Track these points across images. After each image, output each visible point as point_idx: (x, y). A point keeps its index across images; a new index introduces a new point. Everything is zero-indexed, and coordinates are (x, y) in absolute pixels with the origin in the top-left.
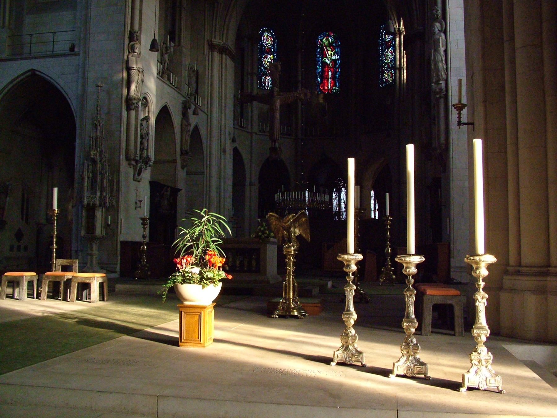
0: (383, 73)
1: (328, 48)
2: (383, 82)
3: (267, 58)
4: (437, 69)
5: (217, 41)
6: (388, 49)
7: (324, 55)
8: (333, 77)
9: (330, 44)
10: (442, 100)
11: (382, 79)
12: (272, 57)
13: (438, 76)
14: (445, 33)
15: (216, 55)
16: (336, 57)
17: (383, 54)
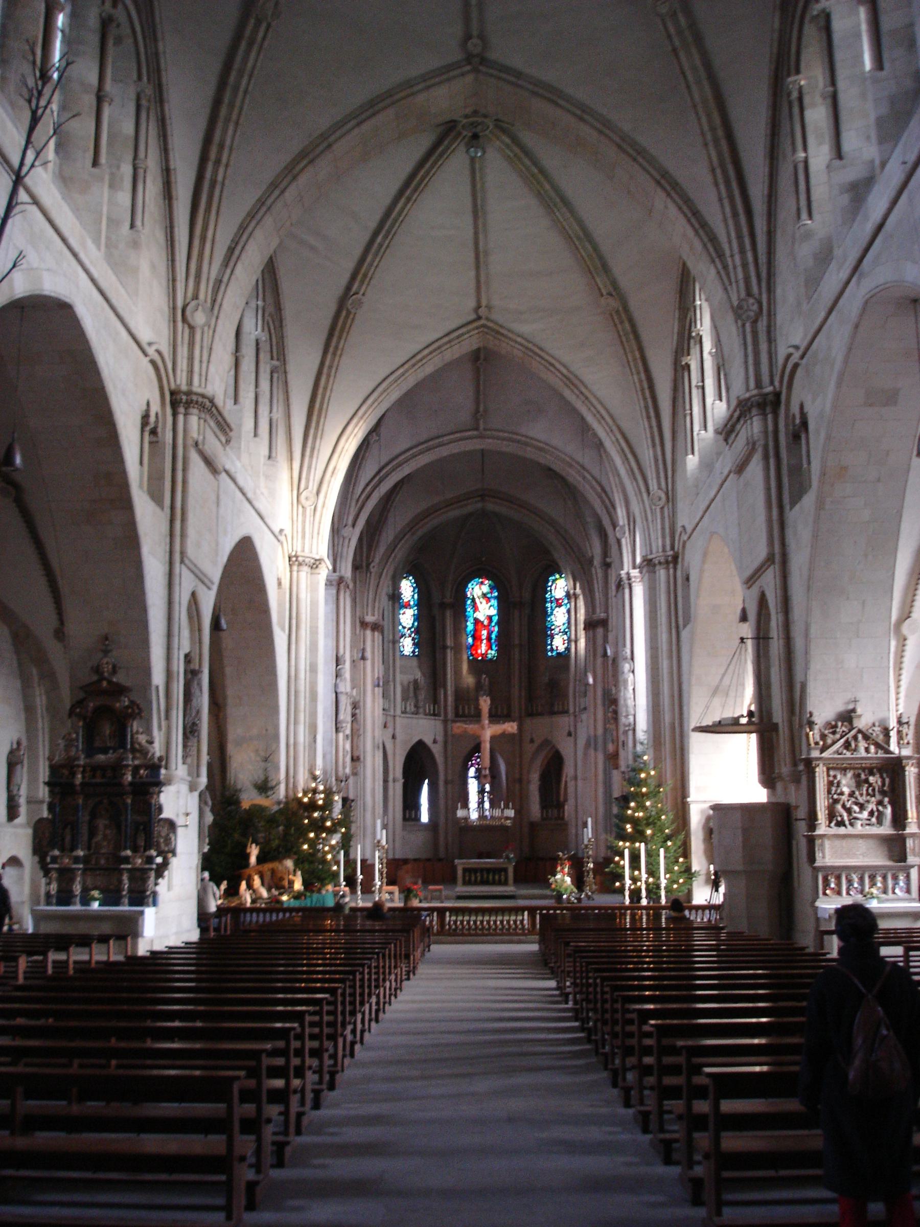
1: (481, 599)
2: (552, 650)
3: (404, 613)
4: (627, 706)
5: (369, 619)
6: (560, 605)
7: (475, 608)
8: (489, 638)
9: (484, 595)
10: (630, 733)
11: (551, 645)
13: (627, 711)
14: (633, 672)
15: (369, 633)
17: (552, 614)
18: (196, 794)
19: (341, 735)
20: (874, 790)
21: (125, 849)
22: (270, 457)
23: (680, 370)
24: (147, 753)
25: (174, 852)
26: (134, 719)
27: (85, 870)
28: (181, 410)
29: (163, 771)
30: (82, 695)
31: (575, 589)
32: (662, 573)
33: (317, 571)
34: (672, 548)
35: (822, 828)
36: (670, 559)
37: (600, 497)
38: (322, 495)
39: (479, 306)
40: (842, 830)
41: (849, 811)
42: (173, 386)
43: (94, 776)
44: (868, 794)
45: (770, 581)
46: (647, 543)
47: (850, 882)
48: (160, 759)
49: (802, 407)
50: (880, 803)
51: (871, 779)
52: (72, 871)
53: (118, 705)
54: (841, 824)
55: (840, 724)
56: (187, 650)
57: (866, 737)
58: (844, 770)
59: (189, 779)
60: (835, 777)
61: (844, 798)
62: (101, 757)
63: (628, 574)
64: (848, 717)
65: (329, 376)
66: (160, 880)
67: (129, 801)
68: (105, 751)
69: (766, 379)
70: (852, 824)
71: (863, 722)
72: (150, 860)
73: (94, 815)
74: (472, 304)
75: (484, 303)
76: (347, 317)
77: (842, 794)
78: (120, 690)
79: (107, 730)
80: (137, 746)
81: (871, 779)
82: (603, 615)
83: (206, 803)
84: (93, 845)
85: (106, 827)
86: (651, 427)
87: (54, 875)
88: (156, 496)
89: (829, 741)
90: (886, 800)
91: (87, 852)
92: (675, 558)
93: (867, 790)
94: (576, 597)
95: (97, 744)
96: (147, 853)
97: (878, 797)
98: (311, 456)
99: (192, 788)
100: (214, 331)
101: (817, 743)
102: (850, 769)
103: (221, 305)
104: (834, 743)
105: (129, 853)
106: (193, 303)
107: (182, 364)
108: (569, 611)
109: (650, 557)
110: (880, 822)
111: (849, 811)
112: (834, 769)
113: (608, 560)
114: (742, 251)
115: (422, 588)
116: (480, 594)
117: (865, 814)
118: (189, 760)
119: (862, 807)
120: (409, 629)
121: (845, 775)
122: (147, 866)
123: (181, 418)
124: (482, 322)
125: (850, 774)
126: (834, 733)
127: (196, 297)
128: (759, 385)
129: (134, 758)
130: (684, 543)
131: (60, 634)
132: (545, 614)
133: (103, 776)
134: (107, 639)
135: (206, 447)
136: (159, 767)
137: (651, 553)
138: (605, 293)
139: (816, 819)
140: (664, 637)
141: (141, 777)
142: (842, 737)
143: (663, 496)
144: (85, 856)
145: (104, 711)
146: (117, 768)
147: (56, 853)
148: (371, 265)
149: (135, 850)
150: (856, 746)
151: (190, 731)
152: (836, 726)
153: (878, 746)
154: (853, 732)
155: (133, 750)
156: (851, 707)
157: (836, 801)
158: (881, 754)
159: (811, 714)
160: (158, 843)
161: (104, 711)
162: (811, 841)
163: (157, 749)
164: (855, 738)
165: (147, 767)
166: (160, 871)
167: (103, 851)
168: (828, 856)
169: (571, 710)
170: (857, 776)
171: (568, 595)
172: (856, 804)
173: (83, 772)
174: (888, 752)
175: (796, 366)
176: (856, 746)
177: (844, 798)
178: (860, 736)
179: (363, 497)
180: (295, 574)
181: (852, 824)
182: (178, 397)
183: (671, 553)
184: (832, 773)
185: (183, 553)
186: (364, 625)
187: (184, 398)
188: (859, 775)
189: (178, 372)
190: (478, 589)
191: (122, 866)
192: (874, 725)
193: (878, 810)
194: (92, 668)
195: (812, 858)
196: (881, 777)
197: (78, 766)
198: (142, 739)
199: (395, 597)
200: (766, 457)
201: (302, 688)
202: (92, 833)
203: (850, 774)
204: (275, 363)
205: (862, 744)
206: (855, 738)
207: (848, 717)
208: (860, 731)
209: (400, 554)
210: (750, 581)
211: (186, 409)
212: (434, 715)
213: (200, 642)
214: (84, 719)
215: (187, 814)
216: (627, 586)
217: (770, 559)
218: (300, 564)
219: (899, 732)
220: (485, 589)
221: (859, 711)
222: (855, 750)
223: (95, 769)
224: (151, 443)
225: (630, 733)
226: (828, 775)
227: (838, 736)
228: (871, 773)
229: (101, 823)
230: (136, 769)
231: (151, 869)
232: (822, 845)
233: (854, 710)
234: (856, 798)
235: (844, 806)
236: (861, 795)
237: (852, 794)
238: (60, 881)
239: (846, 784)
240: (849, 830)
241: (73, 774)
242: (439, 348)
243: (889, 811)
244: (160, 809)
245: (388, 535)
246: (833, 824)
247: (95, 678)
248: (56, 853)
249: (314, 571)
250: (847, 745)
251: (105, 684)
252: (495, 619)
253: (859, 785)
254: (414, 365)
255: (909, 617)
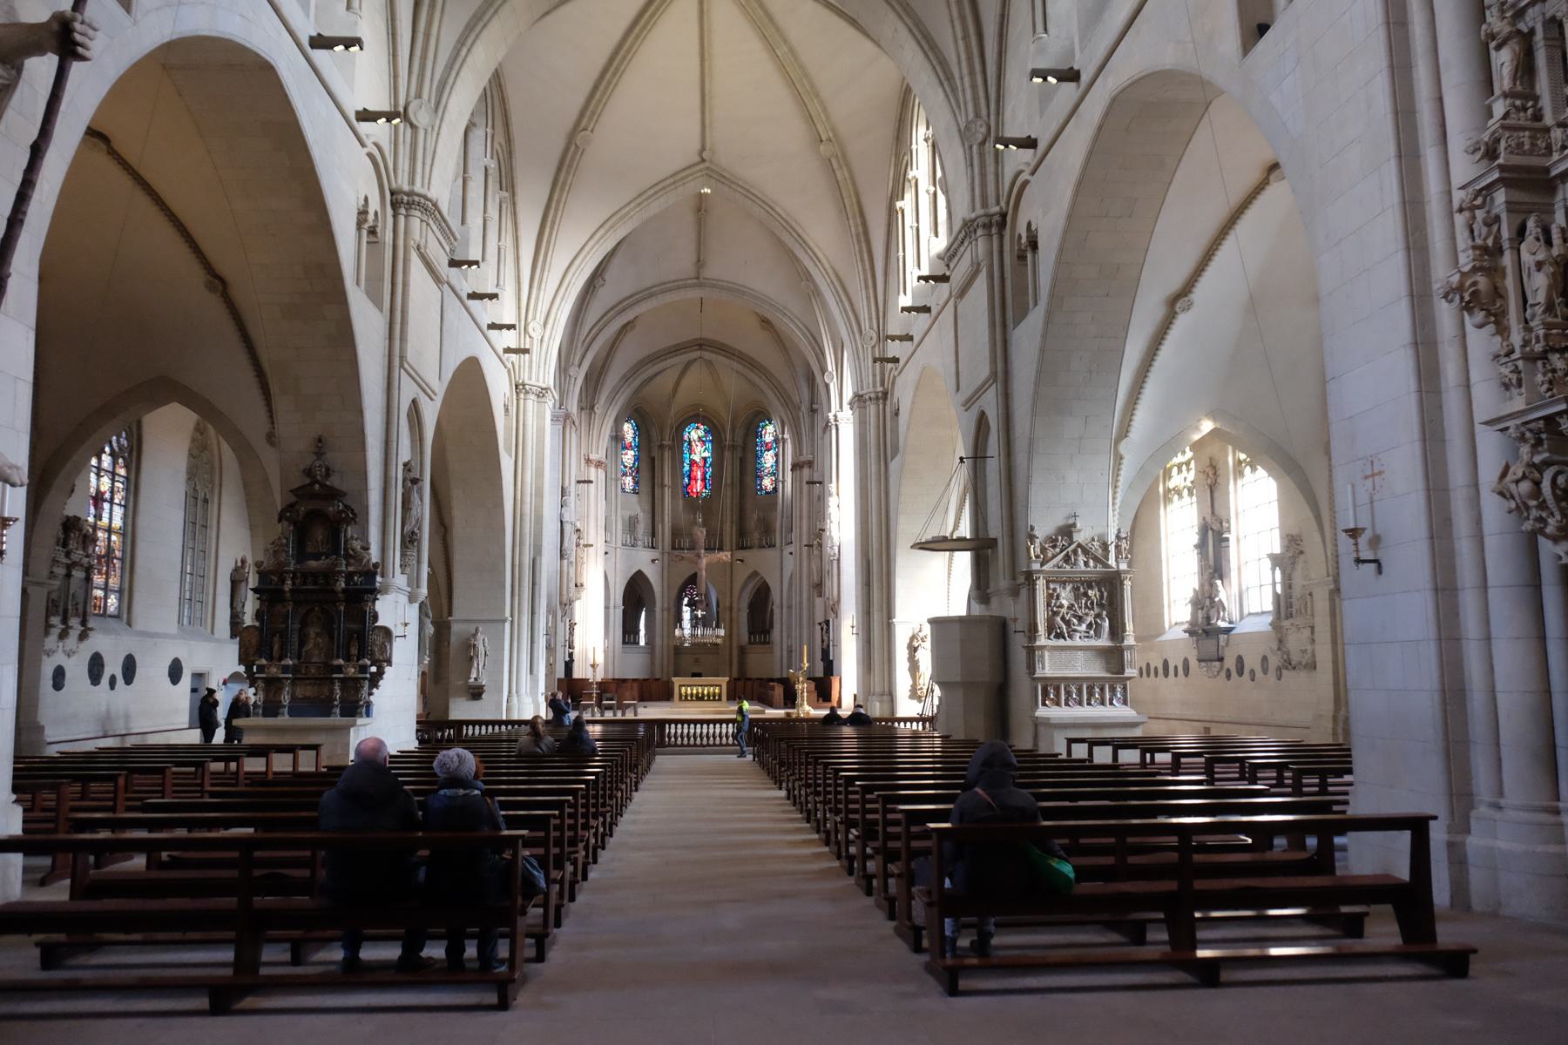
0: (762, 478)
2: (761, 489)
5: (593, 456)
6: (769, 450)
7: (691, 451)
8: (704, 479)
10: (835, 563)
11: (761, 485)
12: (632, 453)
15: (593, 470)
16: (707, 454)
18: (416, 606)
19: (565, 562)
20: (1092, 603)
21: (338, 657)
22: (497, 285)
23: (892, 215)
24: (361, 560)
25: (389, 663)
26: (348, 524)
27: (294, 681)
28: (403, 211)
29: (379, 579)
30: (293, 499)
31: (783, 433)
32: (872, 409)
33: (543, 400)
34: (882, 384)
35: (1042, 641)
36: (880, 395)
37: (810, 344)
38: (549, 326)
39: (703, 149)
40: (1061, 642)
41: (1068, 623)
42: (394, 186)
43: (305, 583)
44: (1086, 607)
45: (990, 403)
46: (859, 380)
47: (1068, 693)
48: (376, 565)
49: (1029, 224)
50: (1098, 616)
51: (1090, 592)
52: (279, 680)
53: (331, 509)
54: (1060, 636)
55: (1060, 538)
56: (406, 459)
57: (1086, 552)
58: (1064, 583)
59: (409, 589)
60: (1054, 590)
61: (1064, 610)
62: (313, 564)
63: (835, 416)
64: (1067, 531)
65: (557, 210)
66: (375, 690)
67: (342, 608)
68: (317, 557)
69: (992, 200)
70: (1070, 637)
71: (1080, 538)
72: (364, 669)
73: (304, 624)
74: (698, 146)
75: (708, 147)
76: (575, 153)
77: (1061, 606)
78: (334, 494)
79: (319, 534)
80: (351, 552)
81: (1090, 592)
82: (810, 457)
83: (427, 616)
84: (304, 654)
85: (317, 634)
86: (864, 270)
87: (261, 684)
88: (375, 297)
89: (1050, 555)
90: (1104, 613)
91: (296, 662)
92: (885, 394)
93: (1086, 604)
94: (784, 441)
95: (309, 550)
96: (361, 662)
97: (1097, 610)
98: (539, 288)
99: (412, 599)
100: (438, 134)
101: (1037, 557)
102: (1069, 582)
103: (445, 107)
104: (1054, 556)
105: (341, 662)
106: (418, 101)
107: (404, 164)
108: (777, 455)
109: (861, 393)
110: (1098, 635)
111: (1068, 623)
112: (1053, 582)
113: (815, 406)
114: (972, 73)
115: (640, 430)
116: (696, 437)
117: (1084, 627)
118: (408, 570)
119: (1080, 619)
120: (631, 468)
121: (1064, 588)
122: (360, 676)
123: (402, 219)
124: (707, 164)
125: (1069, 588)
126: (1054, 547)
127: (419, 96)
128: (985, 204)
129: (347, 565)
130: (895, 378)
131: (271, 438)
132: (757, 457)
133: (315, 583)
134: (320, 441)
135: (428, 251)
136: (376, 573)
137: (862, 389)
138: (824, 138)
139: (1036, 630)
140: (873, 468)
141: (356, 584)
142: (1062, 551)
143: (875, 336)
144: (294, 665)
145: (315, 516)
146: (329, 575)
147: (264, 662)
148: (599, 101)
149: (348, 658)
150: (1075, 560)
151: (410, 540)
152: (1057, 540)
153: (1096, 559)
154: (1073, 547)
155: (347, 556)
156: (1071, 521)
157: (1055, 614)
158: (1099, 568)
159: (1032, 528)
160: (373, 653)
161: (315, 516)
162: (1031, 651)
163: (374, 555)
164: (1075, 552)
165: (360, 574)
166: (375, 681)
167: (314, 660)
168: (1048, 668)
169: (778, 544)
170: (1076, 589)
171: (776, 440)
172: (1075, 616)
173: (292, 579)
174: (1106, 566)
175: (1026, 183)
176: (1075, 560)
177: (1064, 610)
178: (1080, 550)
179: (589, 338)
180: (522, 401)
181: (1070, 637)
182: (399, 197)
183: (881, 389)
184: (1052, 586)
185: (402, 358)
186: (588, 461)
187: (405, 198)
188: (1078, 588)
189: (400, 172)
190: (694, 433)
191: (334, 676)
192: (1093, 540)
193: (1096, 622)
194: (304, 471)
195: (1031, 667)
196: (1100, 591)
197: (288, 572)
198: (357, 545)
199: (617, 438)
200: (991, 276)
201: (527, 510)
202: (302, 643)
203: (1069, 588)
204: (505, 194)
205: (1081, 558)
206: (1075, 552)
207: (1067, 531)
208: (1079, 545)
209: (621, 400)
210: (968, 404)
211: (406, 209)
212: (653, 547)
213: (422, 453)
214: (295, 523)
215: (406, 624)
216: (834, 427)
217: (994, 374)
218: (527, 392)
219: (1117, 547)
220: (701, 433)
221: (1079, 526)
222: (1075, 564)
223: (306, 575)
224: (368, 242)
225: (835, 563)
226: (1048, 588)
227: (1058, 550)
228: (1091, 587)
229: (312, 631)
230: (349, 576)
231: (366, 678)
232: (1042, 656)
233: (1074, 525)
234: (1075, 611)
235: (1063, 619)
236: (1080, 608)
237: (1071, 607)
238: (267, 691)
239: (1066, 597)
240: (1069, 642)
241: (283, 582)
242: (664, 188)
243: (1107, 624)
244: (375, 617)
245: (611, 380)
246: (1052, 637)
247: (307, 481)
248: (264, 662)
249: (540, 400)
250: (1067, 559)
251: (317, 487)
252: (709, 460)
253: (1077, 598)
254: (639, 204)
255: (1126, 436)
